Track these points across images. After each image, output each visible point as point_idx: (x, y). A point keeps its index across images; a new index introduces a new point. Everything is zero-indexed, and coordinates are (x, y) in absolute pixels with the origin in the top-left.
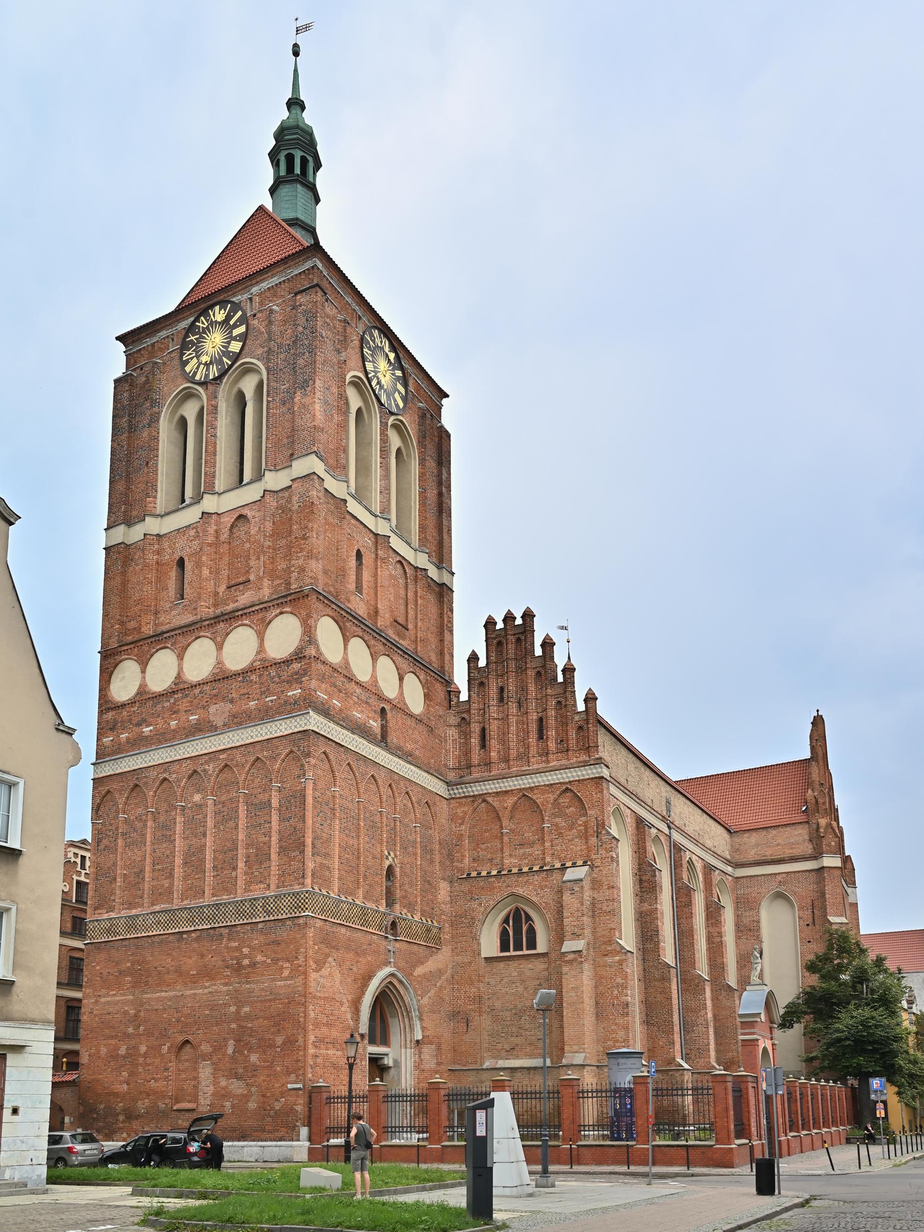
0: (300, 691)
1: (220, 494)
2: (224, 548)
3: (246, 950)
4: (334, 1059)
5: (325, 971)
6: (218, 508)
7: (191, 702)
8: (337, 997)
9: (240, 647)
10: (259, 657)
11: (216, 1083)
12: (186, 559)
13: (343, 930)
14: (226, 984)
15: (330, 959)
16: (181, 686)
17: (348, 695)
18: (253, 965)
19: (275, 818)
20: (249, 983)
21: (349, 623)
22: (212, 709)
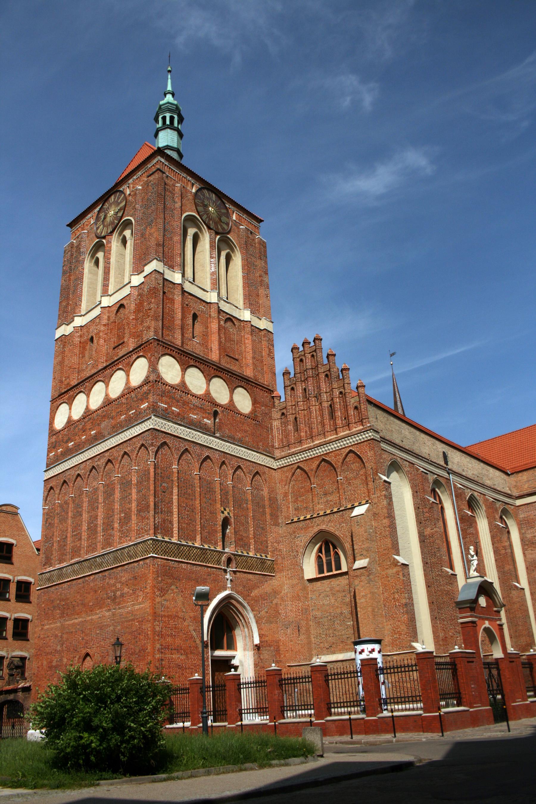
0: (147, 404)
1: (110, 296)
3: (119, 585)
5: (170, 596)
6: (110, 303)
7: (92, 422)
8: (180, 614)
9: (117, 384)
10: (127, 387)
12: (94, 337)
14: (109, 610)
15: (173, 587)
16: (88, 414)
17: (185, 403)
18: (122, 596)
19: (134, 491)
20: (119, 608)
21: (187, 359)
22: (103, 425)
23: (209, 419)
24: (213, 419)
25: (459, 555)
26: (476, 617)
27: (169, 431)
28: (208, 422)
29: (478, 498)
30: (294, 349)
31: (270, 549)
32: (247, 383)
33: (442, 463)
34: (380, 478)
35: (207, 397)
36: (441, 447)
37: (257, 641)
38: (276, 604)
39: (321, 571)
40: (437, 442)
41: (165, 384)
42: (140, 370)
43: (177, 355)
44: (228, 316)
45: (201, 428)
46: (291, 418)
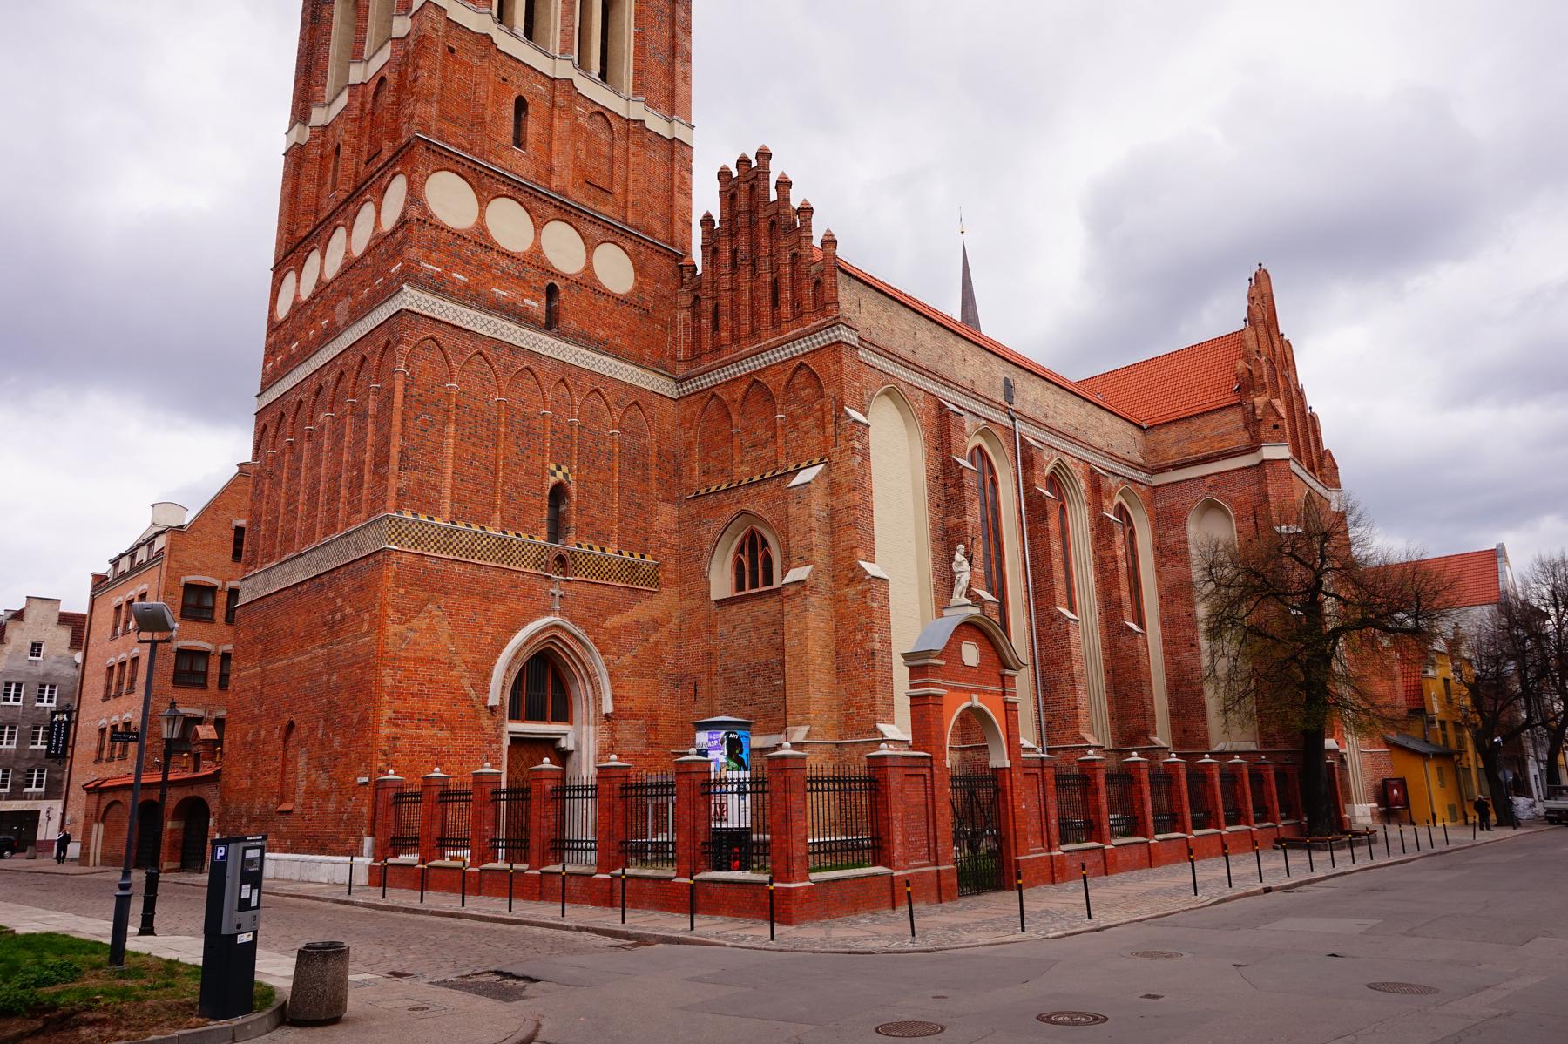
4: (434, 742)
5: (420, 622)
8: (442, 657)
11: (308, 776)
13: (458, 568)
14: (323, 646)
17: (483, 267)
19: (371, 428)
24: (544, 300)
25: (1020, 567)
26: (944, 687)
27: (443, 318)
29: (1072, 468)
30: (724, 174)
31: (653, 543)
32: (617, 233)
33: (1001, 399)
34: (848, 415)
35: (535, 259)
36: (1001, 370)
37: (608, 707)
38: (657, 643)
39: (740, 586)
40: (994, 359)
41: (439, 227)
43: (471, 175)
44: (597, 108)
46: (707, 305)
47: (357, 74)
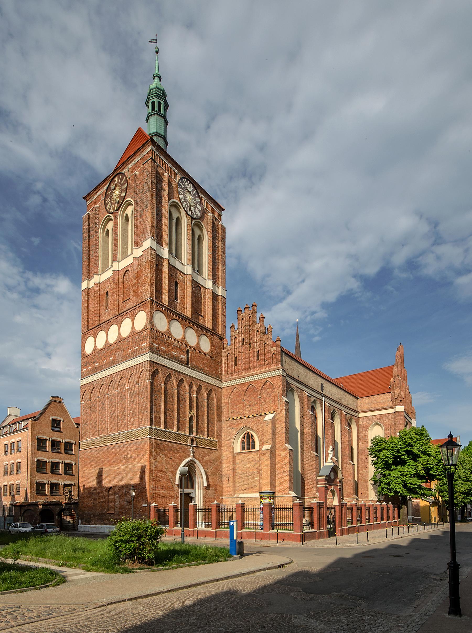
2: (121, 286)
11: (120, 504)
23: (184, 355)
28: (184, 357)
42: (141, 319)
45: (179, 361)
47: (116, 266)
